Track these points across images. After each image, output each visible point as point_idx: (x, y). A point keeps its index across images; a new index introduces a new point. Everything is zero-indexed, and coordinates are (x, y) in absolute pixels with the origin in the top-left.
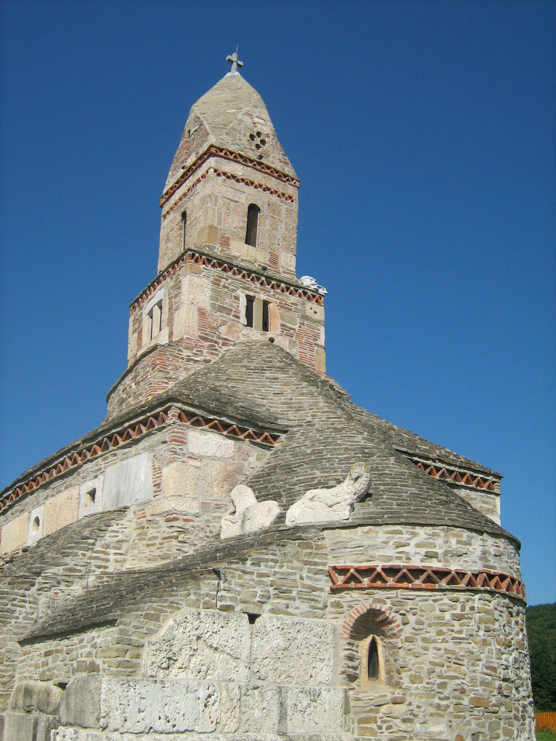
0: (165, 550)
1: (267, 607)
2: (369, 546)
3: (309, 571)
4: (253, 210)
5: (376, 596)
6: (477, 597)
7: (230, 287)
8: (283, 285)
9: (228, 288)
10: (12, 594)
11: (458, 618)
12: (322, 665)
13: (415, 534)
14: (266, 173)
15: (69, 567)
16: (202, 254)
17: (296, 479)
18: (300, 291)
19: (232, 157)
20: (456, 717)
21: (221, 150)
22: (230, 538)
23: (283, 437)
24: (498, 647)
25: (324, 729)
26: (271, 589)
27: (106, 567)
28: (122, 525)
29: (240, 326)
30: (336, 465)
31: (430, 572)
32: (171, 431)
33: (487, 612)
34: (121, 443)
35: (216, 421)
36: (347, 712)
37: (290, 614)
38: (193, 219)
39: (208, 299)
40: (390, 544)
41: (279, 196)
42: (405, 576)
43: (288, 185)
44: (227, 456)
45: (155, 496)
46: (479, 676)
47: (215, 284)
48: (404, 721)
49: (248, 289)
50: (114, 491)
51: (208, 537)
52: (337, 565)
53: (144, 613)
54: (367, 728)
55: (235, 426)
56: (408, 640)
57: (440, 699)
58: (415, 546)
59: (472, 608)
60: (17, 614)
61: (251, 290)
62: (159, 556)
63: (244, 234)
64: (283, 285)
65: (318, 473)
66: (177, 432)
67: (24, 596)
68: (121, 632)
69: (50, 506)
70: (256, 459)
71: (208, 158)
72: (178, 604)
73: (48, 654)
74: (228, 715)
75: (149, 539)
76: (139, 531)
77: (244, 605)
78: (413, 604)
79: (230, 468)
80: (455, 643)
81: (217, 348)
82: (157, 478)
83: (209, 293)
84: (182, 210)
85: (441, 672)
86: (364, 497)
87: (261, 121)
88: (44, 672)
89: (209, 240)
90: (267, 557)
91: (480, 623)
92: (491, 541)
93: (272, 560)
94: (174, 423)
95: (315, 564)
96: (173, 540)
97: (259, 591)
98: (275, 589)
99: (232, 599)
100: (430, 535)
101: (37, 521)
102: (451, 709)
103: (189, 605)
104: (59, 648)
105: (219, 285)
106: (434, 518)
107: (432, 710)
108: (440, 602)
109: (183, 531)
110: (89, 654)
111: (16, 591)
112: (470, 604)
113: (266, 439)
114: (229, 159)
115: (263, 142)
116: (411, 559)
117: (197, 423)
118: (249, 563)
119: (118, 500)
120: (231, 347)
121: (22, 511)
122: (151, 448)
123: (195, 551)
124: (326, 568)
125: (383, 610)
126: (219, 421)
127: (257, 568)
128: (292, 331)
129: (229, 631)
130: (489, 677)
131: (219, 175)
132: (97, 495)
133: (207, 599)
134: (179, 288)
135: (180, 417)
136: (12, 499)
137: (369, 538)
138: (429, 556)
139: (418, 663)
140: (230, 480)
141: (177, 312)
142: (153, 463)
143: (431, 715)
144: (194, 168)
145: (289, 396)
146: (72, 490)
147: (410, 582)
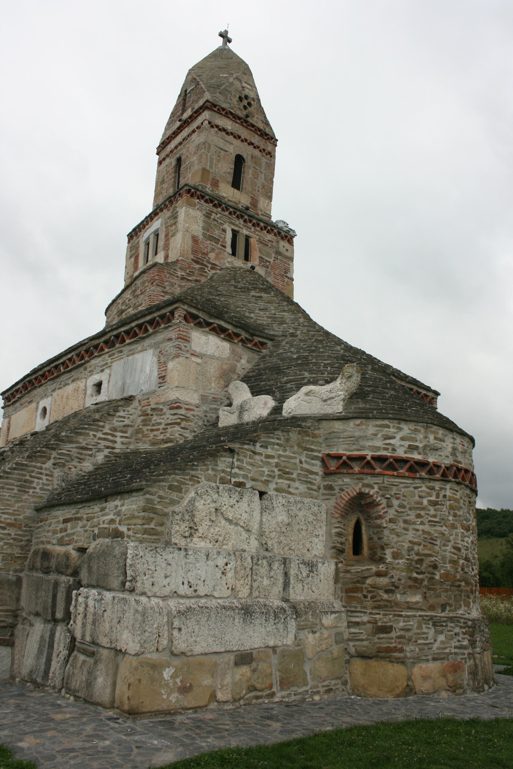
0: (168, 435)
1: (272, 486)
2: (360, 437)
3: (307, 456)
4: (239, 160)
5: (366, 481)
6: (448, 486)
7: (219, 221)
8: (262, 224)
9: (217, 221)
10: (31, 466)
11: (434, 504)
12: (317, 540)
13: (400, 429)
14: (250, 130)
15: (81, 445)
17: (285, 378)
18: (276, 231)
19: (223, 113)
20: (429, 589)
21: (215, 106)
22: (228, 427)
23: (269, 343)
24: (462, 531)
25: (319, 597)
26: (276, 470)
27: (113, 448)
28: (128, 411)
29: (226, 254)
30: (322, 368)
31: (412, 462)
32: (178, 329)
33: (456, 500)
34: (128, 341)
35: (215, 325)
36: (336, 582)
37: (290, 493)
38: (187, 163)
39: (200, 229)
40: (379, 436)
41: (260, 151)
42: (391, 464)
43: (268, 143)
44: (224, 357)
45: (159, 387)
46: (448, 554)
47: (207, 217)
48: (387, 591)
49: (234, 224)
50: (120, 383)
51: (206, 426)
52: (331, 452)
53: (168, 484)
54: (354, 596)
55: (230, 331)
56: (391, 521)
57: (417, 573)
60: (34, 485)
61: (236, 225)
62: (163, 440)
63: (230, 179)
64: (262, 224)
65: (307, 374)
66: (183, 331)
67: (41, 469)
68: (148, 501)
69: (56, 397)
70: (245, 362)
71: (203, 111)
72: (198, 477)
73: (65, 521)
74: (242, 582)
75: (153, 425)
76: (142, 418)
77: (254, 483)
78: (397, 490)
79: (225, 367)
80: (431, 525)
81: (206, 271)
82: (162, 371)
83: (201, 224)
84: (178, 156)
85: (419, 550)
88: (63, 537)
90: (273, 441)
91: (450, 509)
92: (458, 440)
93: (277, 444)
94: (180, 322)
95: (312, 450)
96: (177, 426)
98: (279, 470)
99: (245, 477)
100: (412, 430)
101: (45, 410)
102: (426, 583)
103: (209, 480)
104: (79, 515)
105: (210, 218)
106: (416, 416)
107: (411, 583)
108: (420, 489)
109: (186, 419)
110: (112, 521)
111: (34, 464)
112: (442, 493)
114: (222, 114)
115: (249, 104)
116: (396, 450)
117: (200, 325)
118: (258, 445)
119: (123, 390)
120: (218, 271)
121: (30, 402)
122: (156, 346)
123: (194, 436)
124: (320, 455)
125: (371, 493)
126: (218, 325)
127: (264, 450)
128: (268, 263)
129: (244, 505)
130: (456, 557)
131: (212, 127)
132: (104, 386)
133: (222, 475)
134: (176, 218)
135: (185, 318)
136: (21, 392)
137: (360, 430)
138: (412, 448)
139: (399, 542)
140: (226, 377)
141: (173, 238)
142: (159, 357)
143: (410, 587)
144: (190, 120)
145: (273, 312)
146: (79, 382)
147: (395, 469)
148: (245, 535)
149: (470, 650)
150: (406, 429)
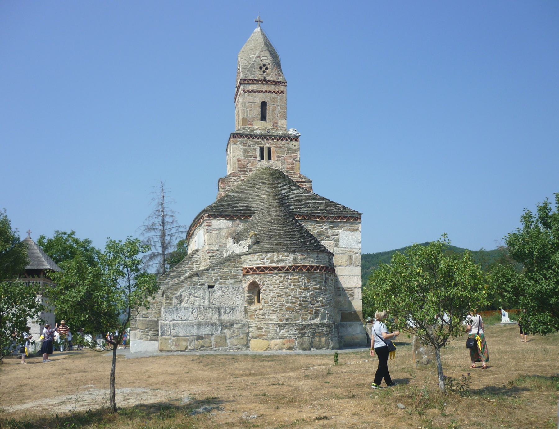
4: (264, 105)
13: (267, 256)
16: (237, 134)
21: (245, 80)
29: (257, 161)
33: (295, 279)
49: (260, 144)
56: (264, 290)
58: (266, 260)
59: (288, 278)
63: (259, 117)
79: (230, 231)
86: (257, 242)
87: (265, 58)
89: (243, 125)
97: (214, 278)
113: (246, 217)
117: (215, 217)
135: (209, 217)
138: (271, 262)
148: (203, 301)
149: (300, 335)
150: (269, 255)
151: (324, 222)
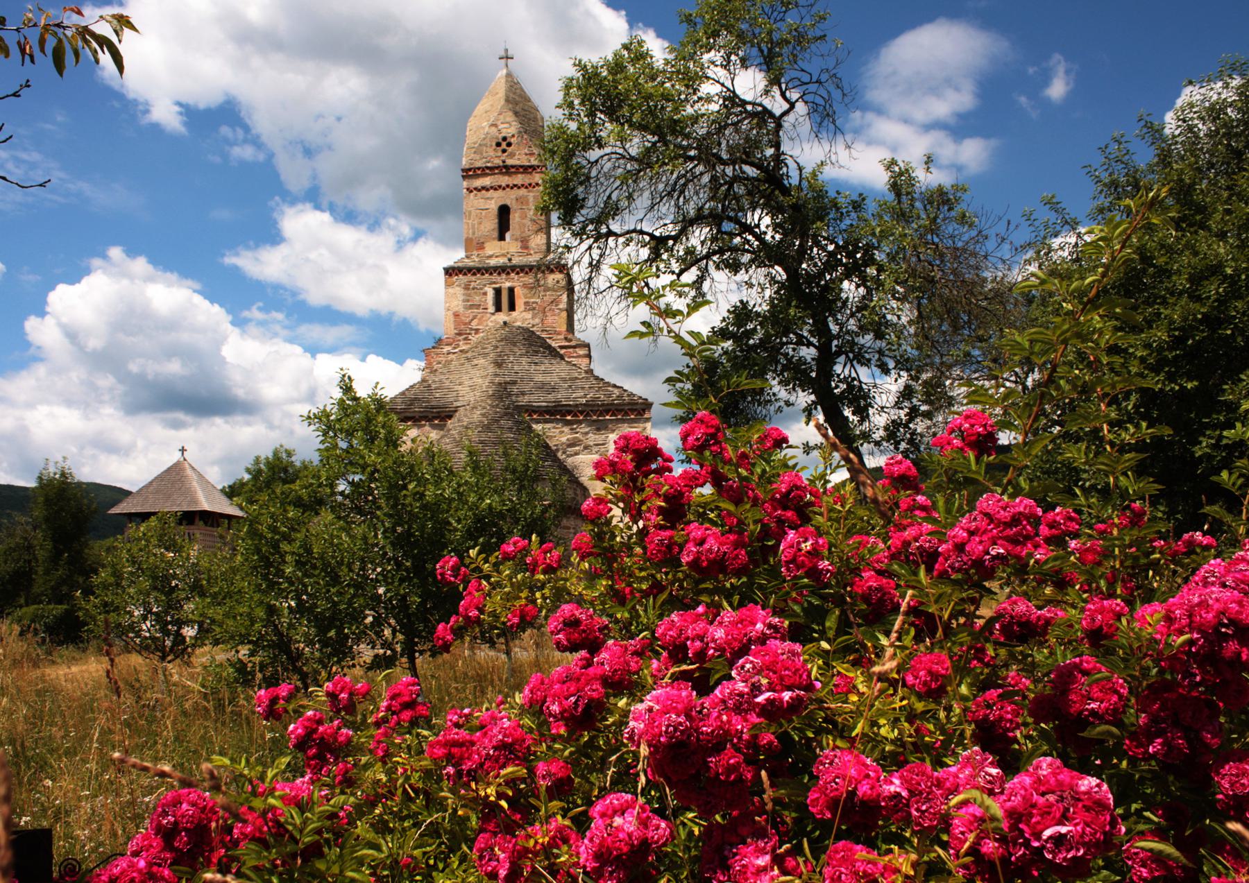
4: (504, 212)
21: (470, 170)
63: (496, 234)
115: (509, 145)
151: (580, 422)
